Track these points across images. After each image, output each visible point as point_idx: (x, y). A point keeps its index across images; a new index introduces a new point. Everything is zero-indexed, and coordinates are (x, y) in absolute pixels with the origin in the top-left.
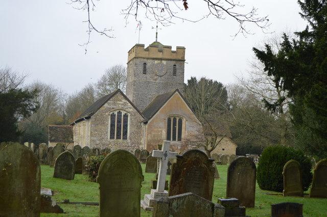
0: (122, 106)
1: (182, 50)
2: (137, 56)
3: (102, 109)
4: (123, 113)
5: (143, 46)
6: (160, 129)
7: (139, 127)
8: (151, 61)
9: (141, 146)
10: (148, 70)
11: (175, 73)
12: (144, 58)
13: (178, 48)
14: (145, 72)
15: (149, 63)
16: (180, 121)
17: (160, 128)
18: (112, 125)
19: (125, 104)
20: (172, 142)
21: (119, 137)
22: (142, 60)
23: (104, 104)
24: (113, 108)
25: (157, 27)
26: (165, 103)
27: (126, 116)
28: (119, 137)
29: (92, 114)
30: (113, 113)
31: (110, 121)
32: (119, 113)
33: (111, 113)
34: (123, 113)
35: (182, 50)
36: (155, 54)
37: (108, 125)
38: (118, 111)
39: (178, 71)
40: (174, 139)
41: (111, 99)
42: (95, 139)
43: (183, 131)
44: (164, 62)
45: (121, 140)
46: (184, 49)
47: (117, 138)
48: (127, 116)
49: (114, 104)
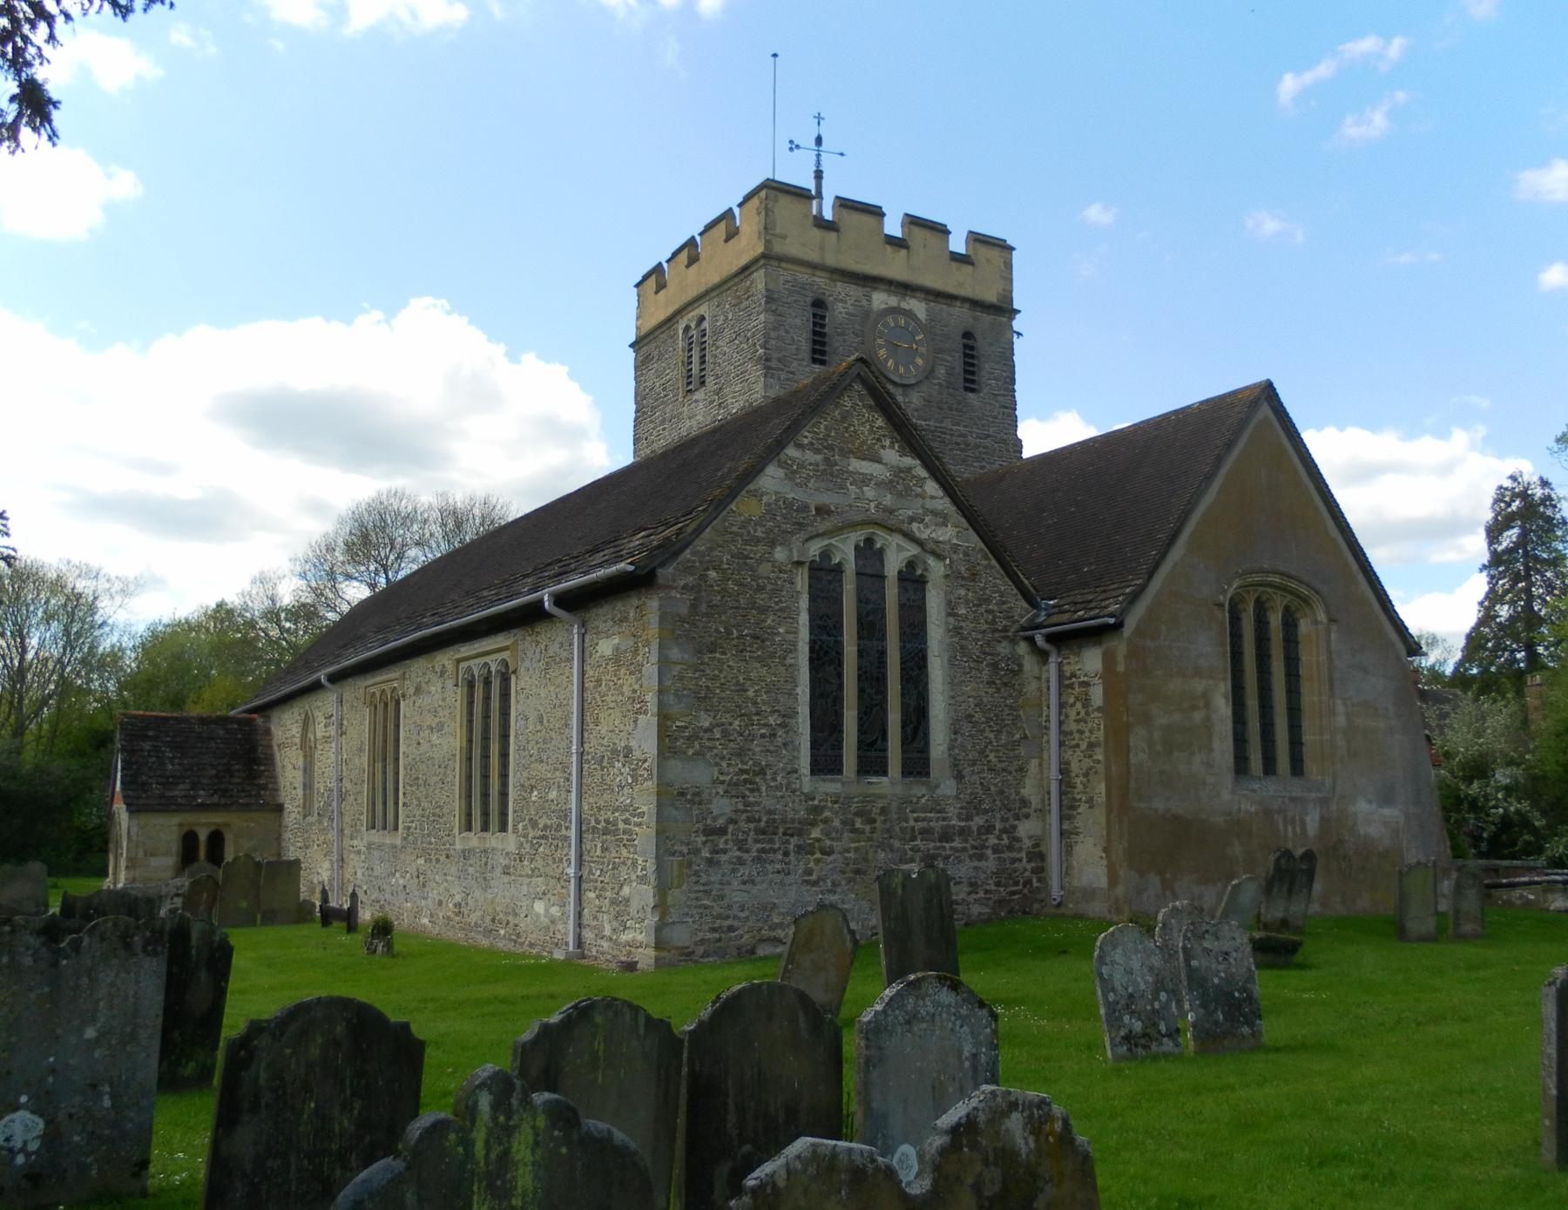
0: (888, 500)
1: (992, 250)
2: (778, 248)
3: (745, 508)
4: (895, 558)
6: (1199, 685)
7: (1007, 676)
8: (855, 292)
9: (1026, 829)
11: (970, 381)
12: (815, 267)
15: (844, 302)
16: (1290, 625)
17: (1198, 673)
18: (824, 656)
19: (899, 482)
20: (1269, 789)
21: (872, 763)
22: (803, 276)
23: (754, 471)
24: (822, 511)
25: (819, 141)
26: (1209, 478)
27: (912, 580)
29: (669, 551)
31: (804, 619)
32: (869, 553)
33: (814, 549)
34: (895, 558)
37: (792, 648)
39: (986, 369)
40: (1269, 767)
42: (700, 775)
43: (1310, 696)
44: (918, 307)
45: (889, 784)
46: (1004, 248)
48: (921, 582)
49: (831, 475)
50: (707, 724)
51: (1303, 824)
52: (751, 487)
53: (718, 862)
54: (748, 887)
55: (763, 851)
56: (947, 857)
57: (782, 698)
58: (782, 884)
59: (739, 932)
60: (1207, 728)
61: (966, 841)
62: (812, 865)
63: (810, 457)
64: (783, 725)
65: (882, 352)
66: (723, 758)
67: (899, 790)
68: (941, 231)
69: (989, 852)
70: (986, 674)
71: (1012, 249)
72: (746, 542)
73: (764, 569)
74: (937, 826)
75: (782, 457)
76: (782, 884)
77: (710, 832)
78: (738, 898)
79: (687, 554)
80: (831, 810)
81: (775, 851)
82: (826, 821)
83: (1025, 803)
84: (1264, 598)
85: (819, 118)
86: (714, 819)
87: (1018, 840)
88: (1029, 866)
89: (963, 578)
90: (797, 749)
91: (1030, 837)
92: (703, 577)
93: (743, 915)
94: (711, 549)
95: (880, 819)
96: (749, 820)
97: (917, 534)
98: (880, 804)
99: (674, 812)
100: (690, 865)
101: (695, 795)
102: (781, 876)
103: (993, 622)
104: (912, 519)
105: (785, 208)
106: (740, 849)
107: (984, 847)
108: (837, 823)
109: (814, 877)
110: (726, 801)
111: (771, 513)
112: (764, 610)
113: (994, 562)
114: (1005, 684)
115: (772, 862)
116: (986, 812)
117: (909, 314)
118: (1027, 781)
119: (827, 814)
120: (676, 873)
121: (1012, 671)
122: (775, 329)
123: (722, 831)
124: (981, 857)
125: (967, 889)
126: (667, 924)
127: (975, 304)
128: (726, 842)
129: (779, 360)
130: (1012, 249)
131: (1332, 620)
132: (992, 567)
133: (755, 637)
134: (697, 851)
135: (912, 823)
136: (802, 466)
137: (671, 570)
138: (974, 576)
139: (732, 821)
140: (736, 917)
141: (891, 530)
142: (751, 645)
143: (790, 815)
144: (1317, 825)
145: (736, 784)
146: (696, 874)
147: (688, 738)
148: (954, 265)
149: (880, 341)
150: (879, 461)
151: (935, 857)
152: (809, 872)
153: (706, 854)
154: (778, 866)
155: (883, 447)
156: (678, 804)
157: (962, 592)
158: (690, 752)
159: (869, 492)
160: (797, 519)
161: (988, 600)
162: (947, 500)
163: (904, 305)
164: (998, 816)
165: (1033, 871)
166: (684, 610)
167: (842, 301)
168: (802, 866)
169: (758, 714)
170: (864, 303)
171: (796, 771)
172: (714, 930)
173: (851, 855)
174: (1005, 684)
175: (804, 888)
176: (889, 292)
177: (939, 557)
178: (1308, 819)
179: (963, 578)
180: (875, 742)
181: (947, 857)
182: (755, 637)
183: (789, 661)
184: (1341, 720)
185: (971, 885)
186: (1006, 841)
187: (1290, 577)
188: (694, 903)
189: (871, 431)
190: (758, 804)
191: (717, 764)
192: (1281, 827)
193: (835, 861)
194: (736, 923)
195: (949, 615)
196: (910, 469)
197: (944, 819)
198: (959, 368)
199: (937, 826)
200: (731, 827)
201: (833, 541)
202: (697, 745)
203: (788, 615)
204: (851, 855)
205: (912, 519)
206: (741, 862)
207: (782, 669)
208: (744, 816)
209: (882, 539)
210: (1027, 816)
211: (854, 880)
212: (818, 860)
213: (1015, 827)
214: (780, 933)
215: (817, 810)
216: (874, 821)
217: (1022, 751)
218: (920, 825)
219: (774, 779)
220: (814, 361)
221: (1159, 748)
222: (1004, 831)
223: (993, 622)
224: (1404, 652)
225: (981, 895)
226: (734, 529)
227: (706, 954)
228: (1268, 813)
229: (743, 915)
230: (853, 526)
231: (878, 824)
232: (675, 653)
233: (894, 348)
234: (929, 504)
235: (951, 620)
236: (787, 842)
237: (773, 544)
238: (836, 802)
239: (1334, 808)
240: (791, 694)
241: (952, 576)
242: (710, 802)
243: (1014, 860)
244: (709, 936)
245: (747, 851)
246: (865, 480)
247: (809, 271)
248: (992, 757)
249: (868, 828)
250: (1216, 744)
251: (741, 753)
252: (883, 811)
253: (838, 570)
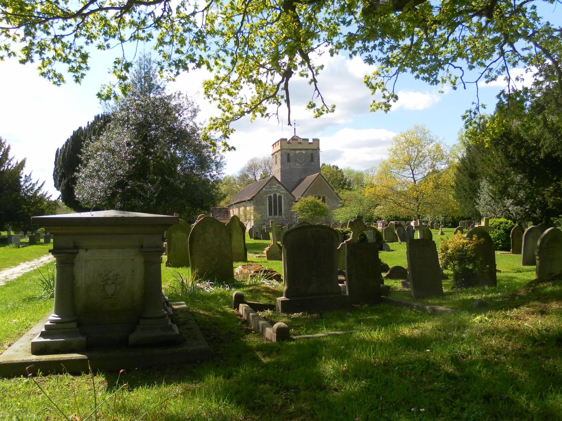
1: (317, 141)
4: (278, 195)
5: (286, 139)
8: (293, 151)
11: (312, 160)
13: (314, 140)
14: (289, 160)
15: (292, 153)
18: (270, 205)
19: (278, 187)
21: (275, 214)
22: (286, 151)
28: (275, 214)
32: (275, 195)
33: (269, 195)
34: (278, 195)
35: (317, 141)
36: (294, 145)
44: (304, 152)
47: (274, 215)
68: (308, 140)
105: (283, 142)
127: (312, 149)
160: (267, 193)
198: (310, 159)
233: (299, 158)
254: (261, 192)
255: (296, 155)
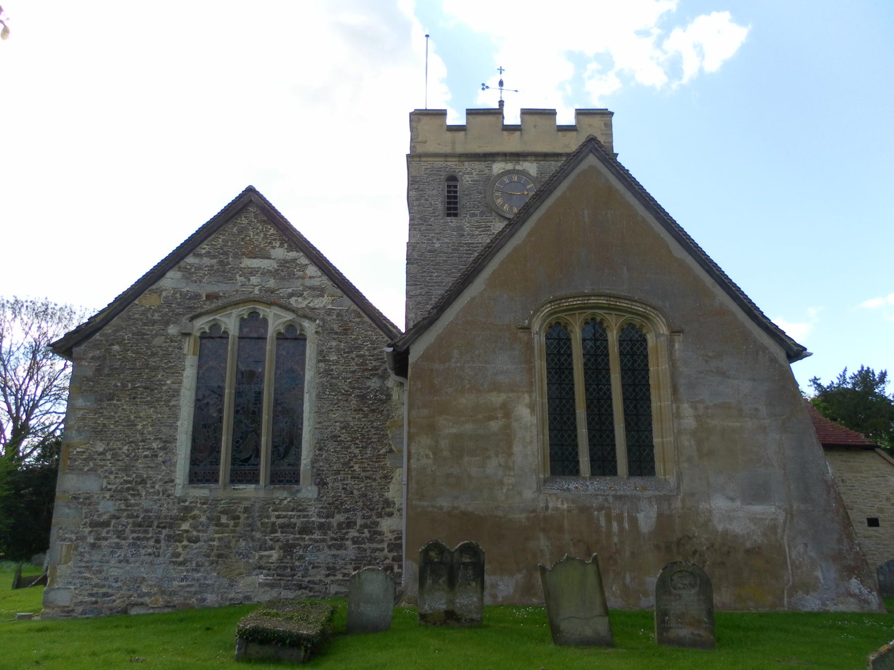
0: (271, 283)
6: (497, 399)
8: (478, 166)
9: (386, 525)
10: (463, 201)
12: (446, 156)
14: (452, 208)
15: (469, 174)
17: (496, 387)
20: (586, 487)
22: (439, 163)
25: (501, 83)
27: (292, 337)
30: (215, 326)
33: (202, 324)
37: (176, 393)
38: (243, 311)
41: (205, 248)
43: (660, 401)
44: (531, 168)
50: (101, 449)
51: (634, 521)
52: (154, 287)
53: (100, 547)
54: (123, 564)
55: (138, 539)
56: (306, 547)
57: (164, 430)
58: (152, 563)
59: (114, 598)
60: (507, 437)
61: (325, 534)
62: (180, 550)
63: (206, 261)
64: (164, 448)
65: (499, 201)
66: (111, 473)
67: (262, 494)
69: (349, 543)
70: (354, 403)
71: (612, 114)
72: (145, 324)
73: (158, 341)
74: (298, 522)
75: (182, 264)
76: (152, 563)
77: (94, 525)
78: (115, 572)
79: (97, 336)
80: (199, 509)
81: (148, 539)
82: (194, 518)
83: (388, 503)
84: (598, 319)
85: (501, 70)
86: (100, 516)
87: (380, 533)
88: (391, 555)
89: (336, 333)
90: (174, 465)
91: (392, 532)
92: (108, 351)
93: (116, 585)
94: (116, 331)
95: (243, 516)
96: (128, 517)
97: (294, 305)
98: (246, 504)
99: (67, 510)
100: (77, 547)
101: (86, 499)
102: (151, 558)
103: (364, 363)
104: (291, 295)
106: (118, 537)
107: (342, 539)
108: (203, 519)
109: (181, 559)
110: (111, 503)
111: (168, 303)
112: (155, 369)
113: (366, 319)
114: (373, 411)
115: (145, 547)
116: (347, 511)
117: (524, 173)
118: (391, 486)
119: (196, 512)
120: (64, 553)
121: (380, 400)
122: (417, 200)
123: (106, 524)
124: (340, 547)
125: (324, 572)
126: (53, 590)
128: (108, 532)
129: (421, 219)
130: (612, 114)
131: (674, 332)
132: (364, 323)
133: (146, 388)
134: (83, 538)
135: (273, 519)
136: (199, 268)
137: (83, 347)
138: (346, 331)
139: (114, 517)
140: (110, 587)
141: (270, 304)
142: (142, 394)
143: (164, 512)
144: (653, 521)
145: (121, 491)
146: (81, 554)
147: (85, 460)
148: (560, 133)
149: (497, 194)
150: (269, 258)
151: (294, 546)
152: (178, 555)
153: (91, 540)
154: (150, 550)
155: (274, 248)
156: (71, 505)
157: (334, 344)
158: (86, 469)
159: (254, 280)
161: (359, 348)
162: (325, 278)
163: (518, 167)
164: (360, 514)
165: (394, 559)
166: (90, 373)
167: (468, 173)
168: (170, 550)
169: (143, 441)
170: (487, 171)
171: (172, 481)
172: (91, 595)
173: (216, 543)
174: (373, 411)
175: (171, 567)
176: (506, 161)
177: (312, 319)
178: (641, 516)
179: (336, 333)
180: (247, 460)
181: (306, 547)
182: (146, 388)
183: (171, 404)
184: (689, 422)
185: (328, 568)
186: (367, 534)
187: (618, 297)
188: (77, 575)
189: (265, 237)
190: (138, 505)
191: (106, 477)
192: (603, 523)
193: (200, 548)
194: (110, 591)
195: (319, 361)
196: (294, 260)
197: (304, 517)
199: (298, 522)
200: (113, 522)
201: (217, 317)
202: (91, 464)
203: (176, 371)
204: (216, 543)
205: (291, 295)
206: (118, 546)
207: (167, 409)
208: (125, 514)
209: (263, 310)
210: (390, 515)
211: (217, 562)
212: (185, 547)
213: (376, 524)
214: (147, 600)
215: (186, 509)
216: (238, 518)
217: (388, 462)
218: (281, 521)
219: (153, 487)
220: (449, 215)
221: (446, 453)
222: (365, 526)
223: (364, 363)
224: (781, 355)
225: (340, 577)
226: (137, 316)
227: (84, 612)
228: (584, 510)
229: (116, 585)
230: (236, 304)
231: (241, 520)
232: (80, 402)
234: (308, 283)
235: (322, 365)
236: (160, 533)
237: (167, 323)
238: (204, 504)
239: (678, 504)
240: (173, 427)
241: (325, 331)
242: (98, 504)
243: (375, 550)
244: (87, 599)
245: (125, 539)
246: (253, 272)
247: (443, 159)
248: (356, 467)
249: (232, 523)
250: (517, 449)
251: (126, 469)
252: (246, 510)
253: (225, 336)
254: (149, 300)
255: (489, 181)
